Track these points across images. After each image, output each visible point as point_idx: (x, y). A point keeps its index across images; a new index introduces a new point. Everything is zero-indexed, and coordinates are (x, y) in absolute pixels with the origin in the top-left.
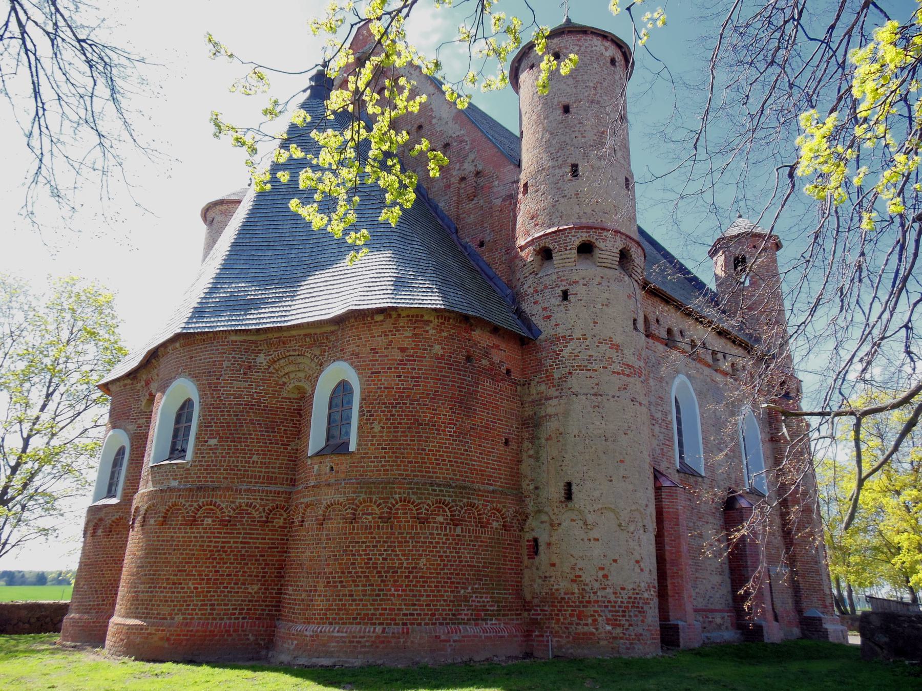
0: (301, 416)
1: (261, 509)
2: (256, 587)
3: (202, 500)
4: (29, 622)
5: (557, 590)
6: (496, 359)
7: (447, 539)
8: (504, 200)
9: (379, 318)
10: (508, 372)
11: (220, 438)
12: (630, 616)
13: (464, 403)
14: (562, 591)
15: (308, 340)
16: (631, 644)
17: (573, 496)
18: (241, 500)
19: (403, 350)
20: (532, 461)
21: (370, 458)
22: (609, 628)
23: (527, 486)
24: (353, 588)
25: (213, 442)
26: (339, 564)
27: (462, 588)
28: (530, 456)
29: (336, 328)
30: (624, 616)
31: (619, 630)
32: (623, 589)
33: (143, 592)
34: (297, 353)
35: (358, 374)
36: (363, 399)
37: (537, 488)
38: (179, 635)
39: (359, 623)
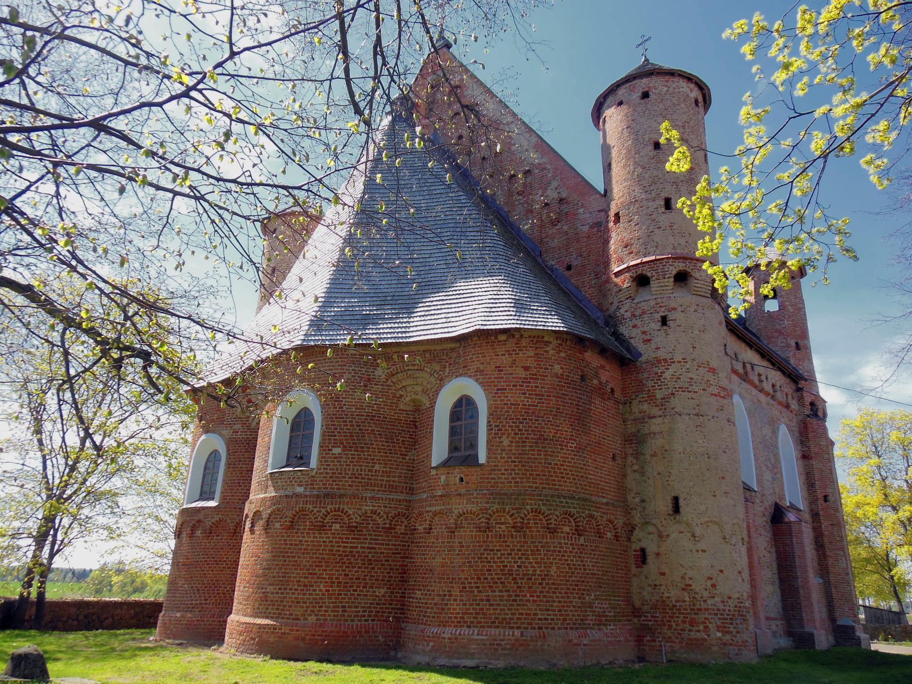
0: (416, 427)
1: (385, 516)
2: (383, 591)
3: (330, 506)
4: (77, 619)
5: (668, 598)
6: (603, 379)
7: (574, 549)
8: (591, 227)
9: (502, 337)
10: (612, 390)
11: (345, 447)
12: (737, 624)
13: (581, 419)
14: (673, 599)
15: (427, 355)
16: (739, 650)
17: (681, 510)
18: (367, 508)
19: (526, 369)
20: (637, 475)
21: (500, 470)
22: (719, 634)
23: (633, 499)
24: (490, 594)
25: (337, 451)
26: (475, 570)
27: (588, 595)
28: (634, 471)
29: (458, 345)
30: (731, 624)
31: (728, 637)
32: (730, 598)
33: (272, 593)
34: (416, 368)
35: (485, 390)
36: (491, 414)
37: (643, 501)
38: (314, 635)
39: (498, 627)
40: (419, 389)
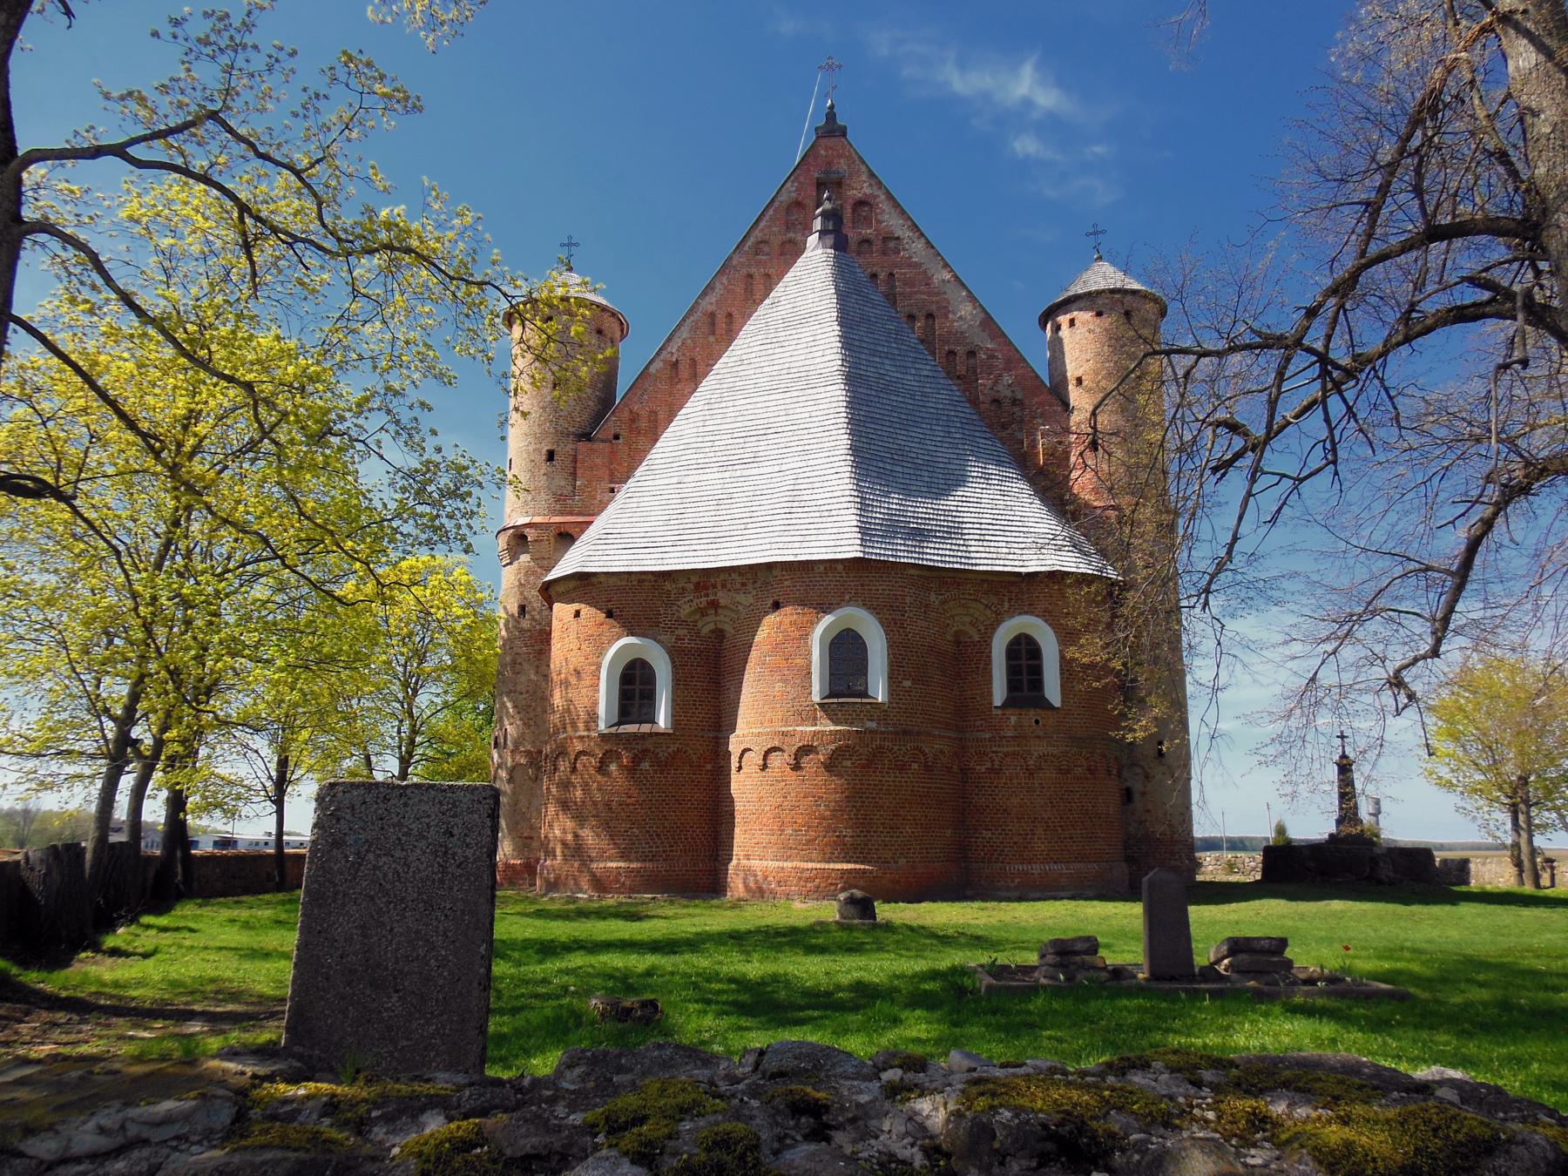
40: (968, 619)
